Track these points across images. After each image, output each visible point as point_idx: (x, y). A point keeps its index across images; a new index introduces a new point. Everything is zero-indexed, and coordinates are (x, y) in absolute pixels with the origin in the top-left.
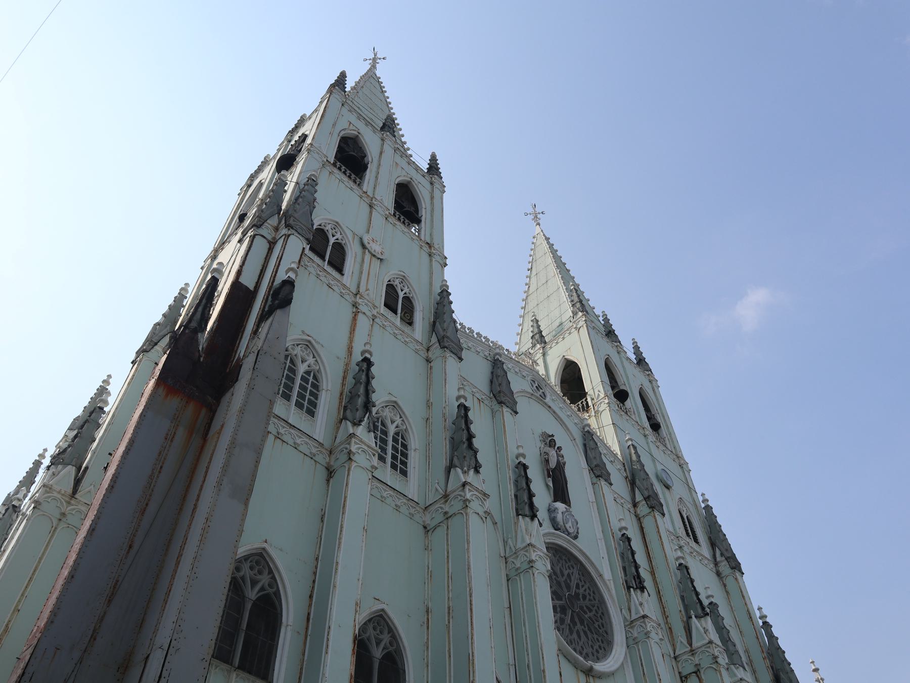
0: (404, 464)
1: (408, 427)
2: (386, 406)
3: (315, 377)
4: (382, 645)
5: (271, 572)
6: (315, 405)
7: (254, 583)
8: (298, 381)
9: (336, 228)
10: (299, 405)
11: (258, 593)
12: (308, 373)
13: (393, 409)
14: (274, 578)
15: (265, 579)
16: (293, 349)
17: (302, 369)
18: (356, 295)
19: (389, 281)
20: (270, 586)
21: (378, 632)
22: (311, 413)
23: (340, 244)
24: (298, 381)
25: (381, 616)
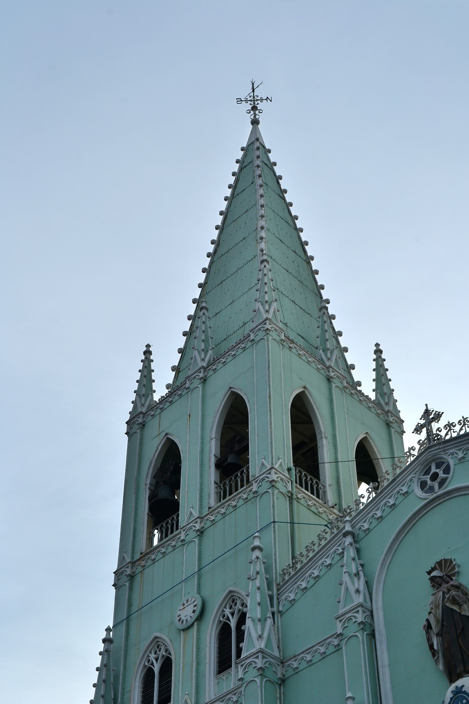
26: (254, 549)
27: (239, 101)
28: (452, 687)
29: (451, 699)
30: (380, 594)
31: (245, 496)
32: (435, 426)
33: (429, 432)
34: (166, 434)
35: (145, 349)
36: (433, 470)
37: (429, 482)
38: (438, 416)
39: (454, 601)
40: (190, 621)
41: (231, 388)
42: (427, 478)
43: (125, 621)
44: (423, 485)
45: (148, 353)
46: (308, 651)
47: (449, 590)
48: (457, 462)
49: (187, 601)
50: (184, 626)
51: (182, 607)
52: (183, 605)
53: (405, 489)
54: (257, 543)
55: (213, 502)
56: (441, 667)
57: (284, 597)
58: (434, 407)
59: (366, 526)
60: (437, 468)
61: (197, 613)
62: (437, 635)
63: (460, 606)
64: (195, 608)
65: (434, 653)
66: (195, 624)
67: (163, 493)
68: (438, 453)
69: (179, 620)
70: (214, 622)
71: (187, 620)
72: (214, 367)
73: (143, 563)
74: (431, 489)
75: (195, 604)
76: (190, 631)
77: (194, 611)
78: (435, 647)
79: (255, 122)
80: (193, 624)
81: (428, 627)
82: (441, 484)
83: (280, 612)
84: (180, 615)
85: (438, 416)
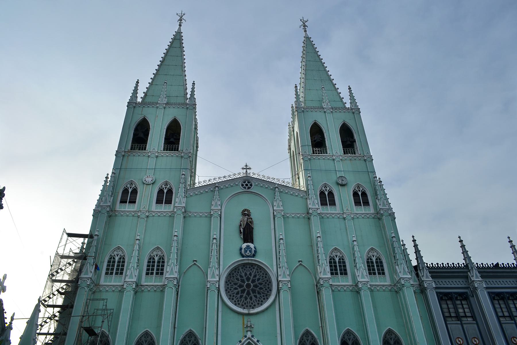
0: (383, 270)
1: (380, 255)
2: (369, 252)
3: (343, 259)
4: (393, 339)
5: (352, 334)
6: (345, 270)
7: (349, 339)
8: (338, 264)
9: (326, 186)
10: (341, 274)
11: (352, 341)
12: (340, 259)
13: (372, 251)
14: (354, 335)
15: (352, 337)
16: (332, 254)
17: (337, 260)
18: (343, 213)
19: (354, 191)
20: (354, 338)
21: (390, 335)
22: (346, 274)
23: (330, 192)
24: (338, 264)
25: (389, 330)
26: (183, 174)
27: (177, 14)
28: (246, 244)
29: (246, 247)
30: (224, 209)
31: (177, 155)
32: (248, 171)
33: (246, 171)
34: (145, 116)
35: (137, 81)
36: (247, 183)
37: (245, 186)
38: (250, 169)
39: (251, 222)
40: (150, 183)
41: (175, 117)
42: (244, 184)
43: (119, 169)
44: (242, 185)
45: (138, 82)
46: (196, 213)
47: (249, 219)
48: (255, 185)
49: (149, 176)
50: (147, 183)
51: (147, 177)
52: (147, 176)
53: (237, 184)
54: (184, 173)
55: (162, 150)
56: (242, 237)
57: (188, 193)
58: (250, 166)
59: (222, 187)
60: (248, 183)
61: (153, 182)
62: (243, 228)
63: (251, 224)
64: (152, 180)
65: (241, 233)
66: (151, 184)
67: (141, 135)
68: (249, 179)
69: (145, 180)
70: (158, 187)
71: (148, 182)
72: (169, 106)
73: (129, 154)
74: (245, 188)
75: (153, 178)
76: (149, 186)
77: (152, 181)
78: (242, 231)
79: (180, 25)
80: (151, 184)
81: (241, 225)
82: (249, 188)
83: (186, 196)
84: (145, 179)
85: (250, 169)
